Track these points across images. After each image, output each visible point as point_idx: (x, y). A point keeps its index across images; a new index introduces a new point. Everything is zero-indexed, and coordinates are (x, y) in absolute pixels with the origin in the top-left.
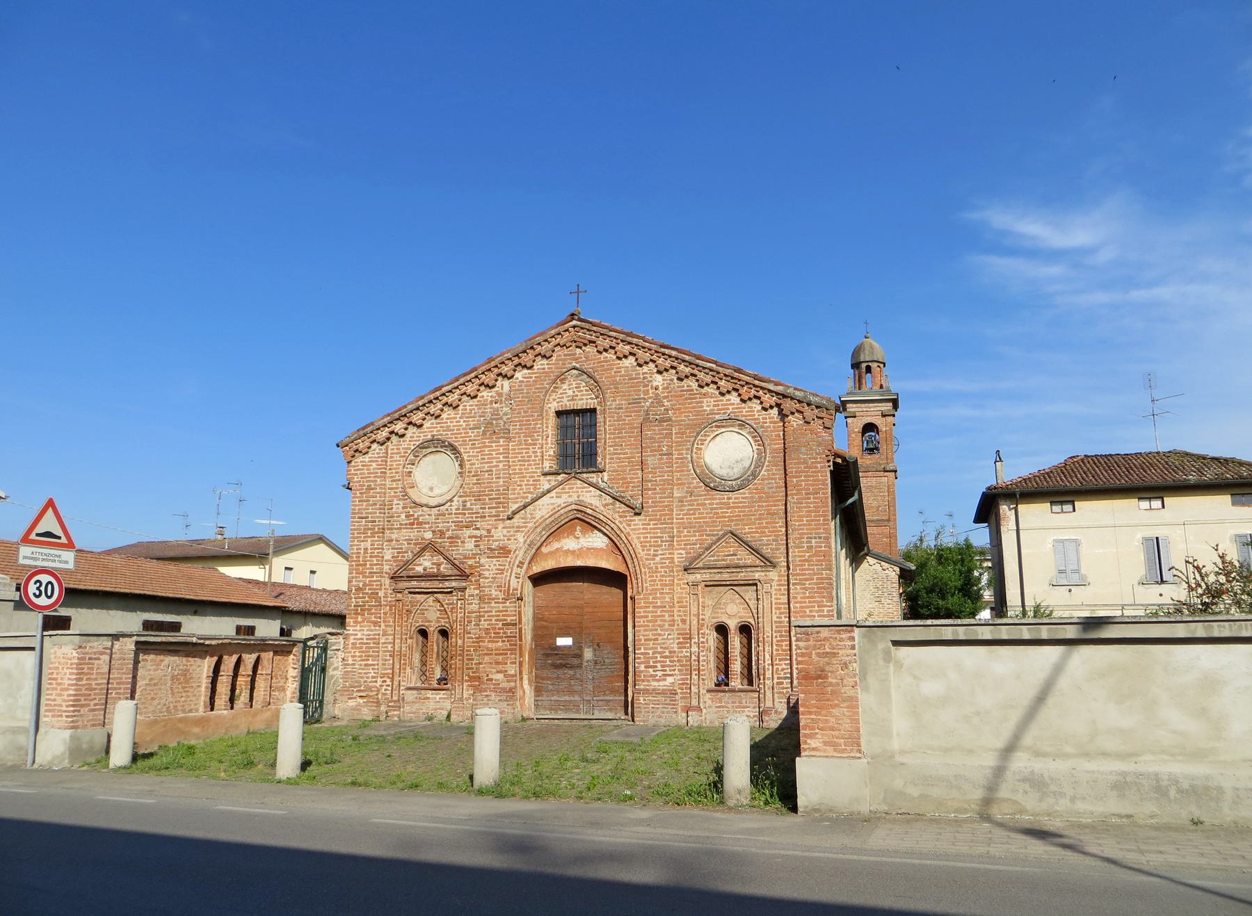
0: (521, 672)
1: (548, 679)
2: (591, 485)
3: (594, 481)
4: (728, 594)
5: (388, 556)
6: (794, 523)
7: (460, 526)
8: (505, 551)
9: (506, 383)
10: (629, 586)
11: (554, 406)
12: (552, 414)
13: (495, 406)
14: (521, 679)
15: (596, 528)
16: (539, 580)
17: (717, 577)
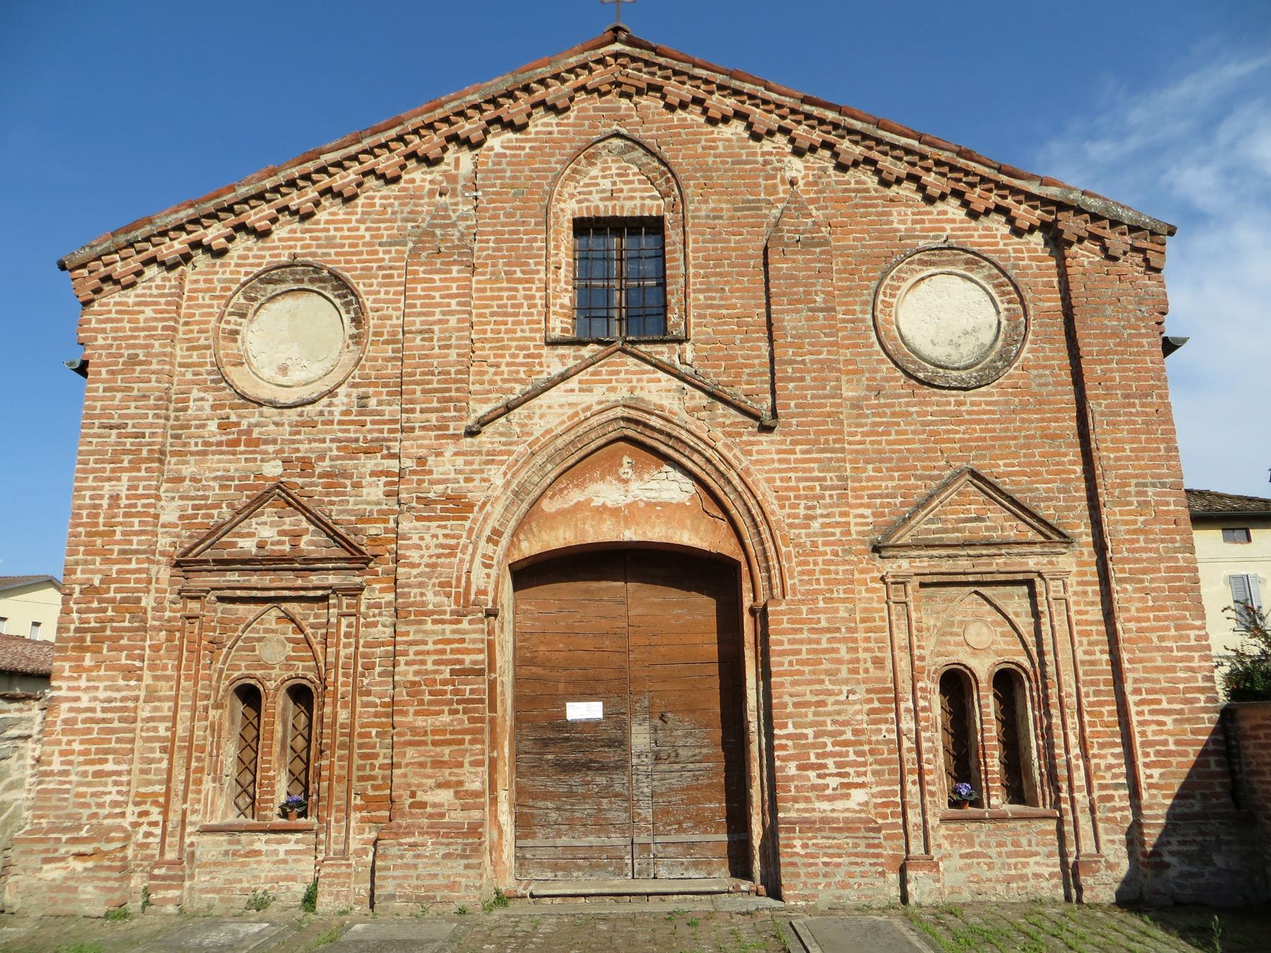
0: (493, 786)
1: (545, 796)
2: (659, 366)
3: (665, 358)
4: (965, 602)
5: (170, 514)
6: (1105, 454)
8: (458, 506)
9: (466, 157)
10: (746, 585)
11: (569, 208)
12: (567, 225)
14: (494, 801)
16: (528, 574)
17: (947, 566)
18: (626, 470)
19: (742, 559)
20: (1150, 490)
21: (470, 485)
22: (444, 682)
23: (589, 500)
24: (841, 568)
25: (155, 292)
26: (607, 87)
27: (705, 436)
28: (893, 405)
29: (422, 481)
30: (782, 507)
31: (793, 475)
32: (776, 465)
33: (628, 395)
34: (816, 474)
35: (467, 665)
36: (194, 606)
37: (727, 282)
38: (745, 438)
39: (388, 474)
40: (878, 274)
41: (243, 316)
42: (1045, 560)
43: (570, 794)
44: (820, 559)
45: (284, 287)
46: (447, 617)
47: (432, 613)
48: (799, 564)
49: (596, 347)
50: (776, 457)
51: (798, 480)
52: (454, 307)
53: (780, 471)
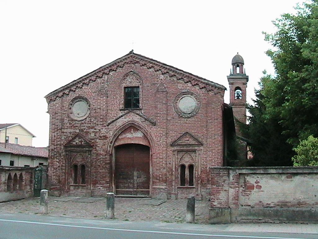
2: (137, 114)
3: (138, 113)
7: (89, 128)
8: (105, 137)
9: (106, 77)
10: (150, 151)
11: (124, 85)
12: (123, 88)
13: (102, 84)
18: (132, 132)
19: (150, 147)
20: (216, 136)
21: (107, 134)
23: (126, 137)
25: (58, 102)
26: (129, 63)
28: (175, 121)
31: (158, 133)
33: (132, 119)
36: (67, 153)
37: (149, 99)
39: (95, 132)
40: (175, 97)
41: (72, 105)
42: (198, 147)
43: (124, 182)
44: (161, 147)
45: (78, 100)
49: (127, 110)
51: (159, 134)
52: (104, 104)
53: (156, 132)
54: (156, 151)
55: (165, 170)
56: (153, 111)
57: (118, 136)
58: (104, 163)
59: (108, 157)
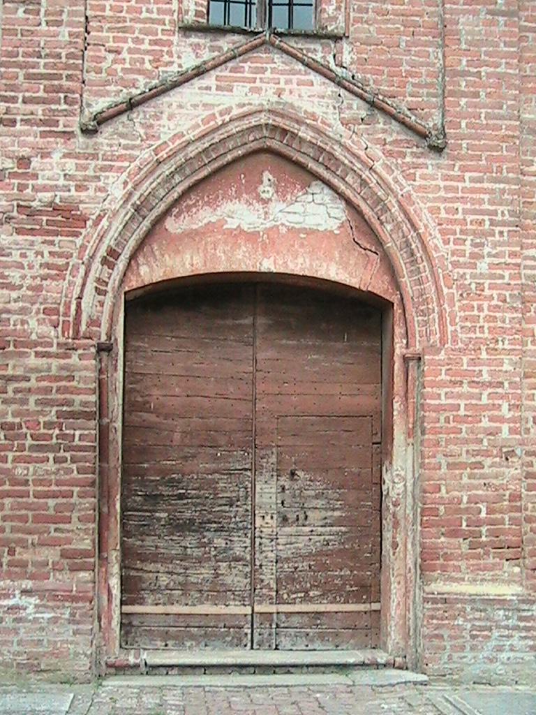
0: (101, 544)
3: (318, 57)
8: (67, 218)
10: (399, 330)
15: (317, 177)
18: (266, 189)
19: (395, 299)
21: (83, 195)
22: (49, 425)
23: (222, 222)
24: (508, 315)
27: (362, 153)
29: (24, 187)
30: (446, 242)
31: (460, 206)
32: (442, 193)
34: (486, 206)
35: (77, 408)
38: (408, 159)
46: (54, 349)
47: (36, 344)
48: (462, 309)
49: (236, 38)
50: (442, 184)
51: (465, 212)
53: (445, 200)
54: (450, 328)
55: (513, 471)
56: (417, 54)
57: (167, 212)
58: (52, 416)
59: (84, 365)
